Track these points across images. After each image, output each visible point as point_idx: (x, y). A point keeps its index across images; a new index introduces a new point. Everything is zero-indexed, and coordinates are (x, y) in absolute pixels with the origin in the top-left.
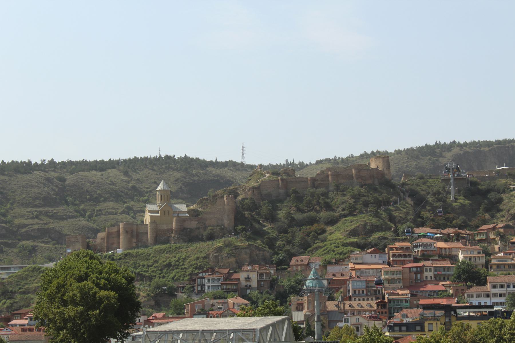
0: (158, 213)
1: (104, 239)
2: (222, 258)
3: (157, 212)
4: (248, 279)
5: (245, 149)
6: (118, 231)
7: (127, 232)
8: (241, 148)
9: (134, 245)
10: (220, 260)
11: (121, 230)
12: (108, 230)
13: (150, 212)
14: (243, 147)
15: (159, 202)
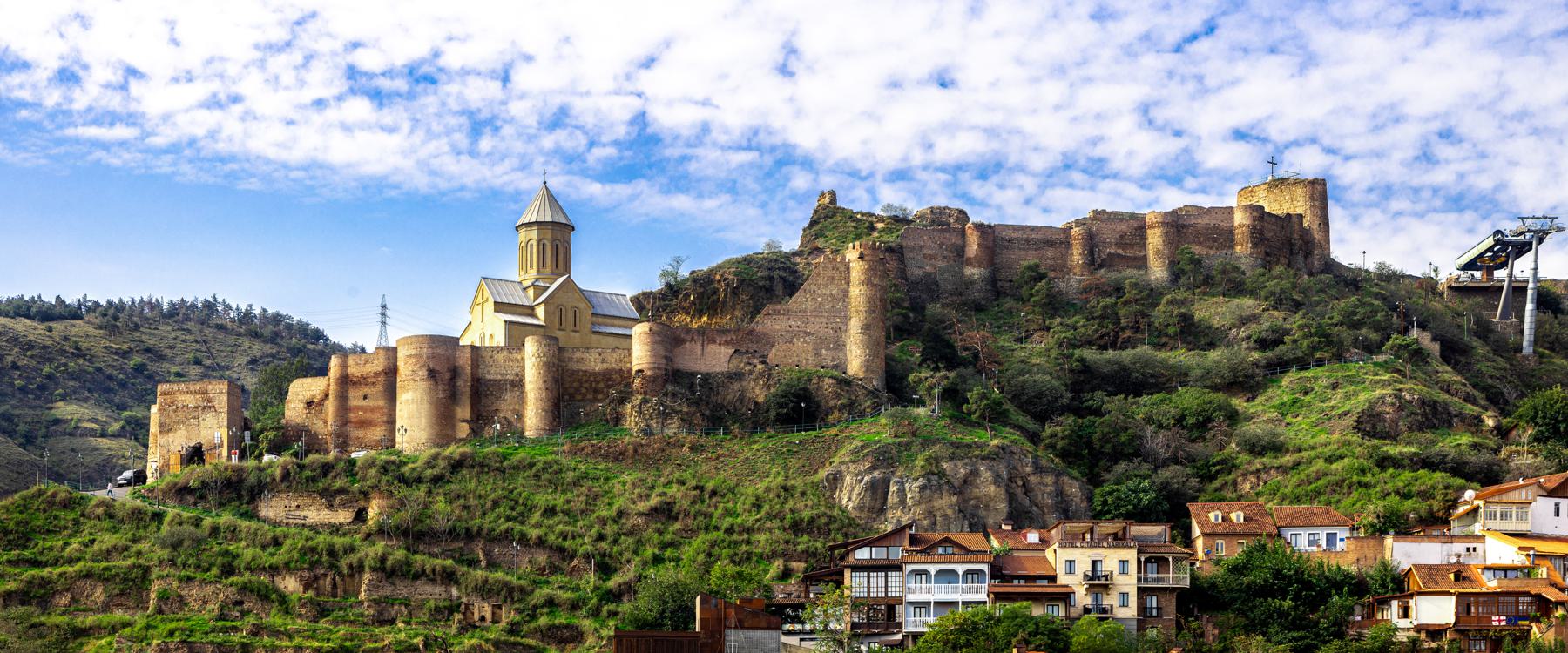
0: (533, 315)
1: (321, 402)
2: (902, 493)
3: (530, 310)
4: (1098, 582)
5: (388, 313)
6: (391, 372)
7: (432, 374)
8: (380, 310)
9: (463, 430)
10: (892, 499)
11: (405, 369)
12: (344, 366)
13: (500, 307)
14: (384, 307)
15: (533, 273)
